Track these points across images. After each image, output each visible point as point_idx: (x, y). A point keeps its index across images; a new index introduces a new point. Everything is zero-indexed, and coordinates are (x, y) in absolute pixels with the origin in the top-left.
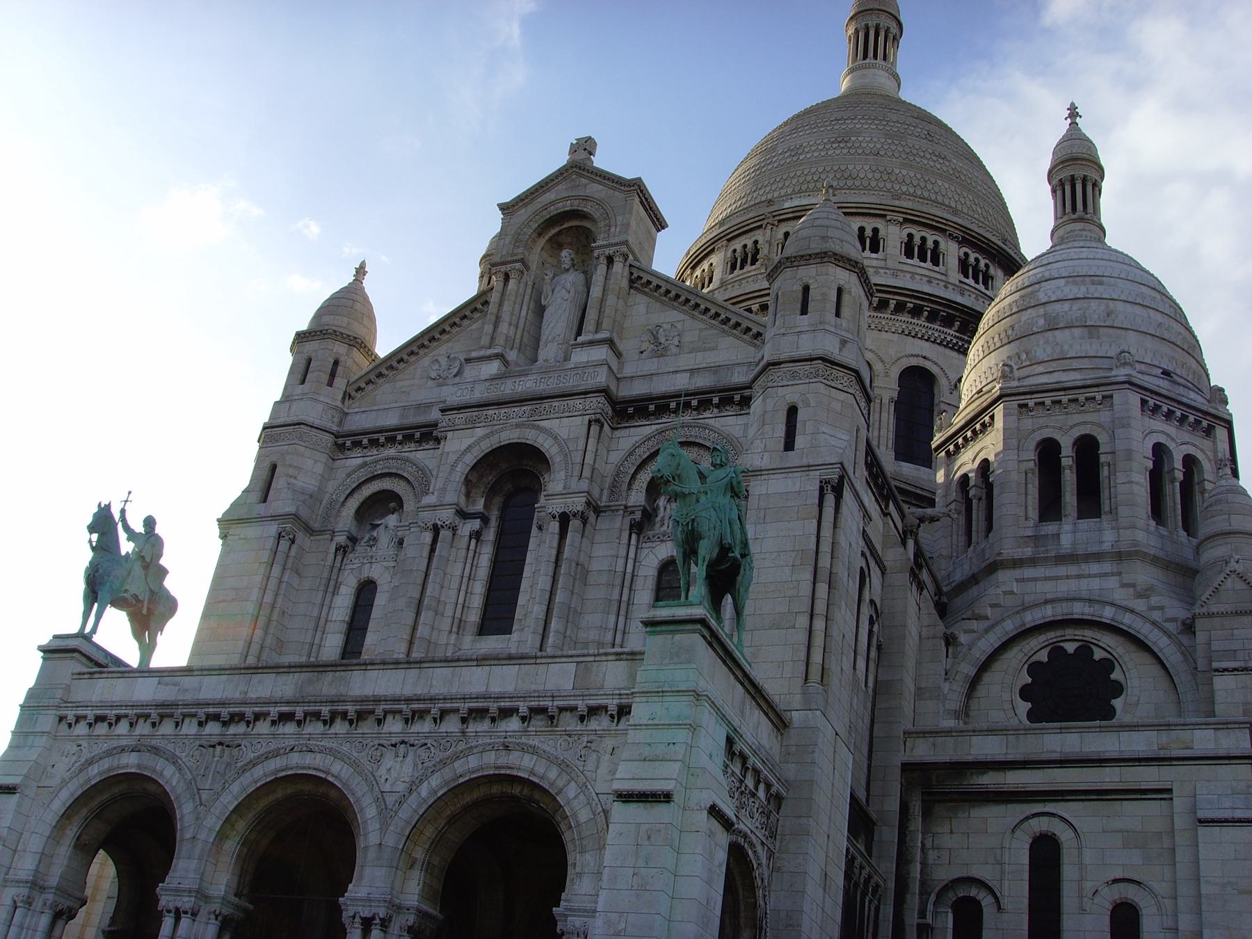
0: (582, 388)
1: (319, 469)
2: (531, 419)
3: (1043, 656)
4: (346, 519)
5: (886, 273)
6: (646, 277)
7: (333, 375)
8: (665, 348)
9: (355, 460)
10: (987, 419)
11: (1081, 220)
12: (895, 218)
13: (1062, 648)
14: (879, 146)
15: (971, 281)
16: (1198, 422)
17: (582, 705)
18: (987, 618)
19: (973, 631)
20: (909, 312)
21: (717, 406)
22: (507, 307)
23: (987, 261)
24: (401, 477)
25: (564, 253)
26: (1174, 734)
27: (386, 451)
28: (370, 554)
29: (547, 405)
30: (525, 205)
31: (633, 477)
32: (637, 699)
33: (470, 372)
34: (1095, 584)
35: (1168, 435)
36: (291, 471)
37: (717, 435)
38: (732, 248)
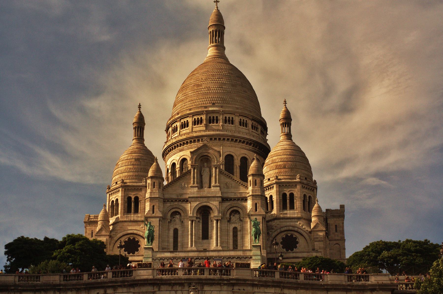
1: (162, 206)
3: (284, 236)
6: (223, 172)
7: (160, 187)
9: (168, 204)
10: (272, 187)
13: (288, 235)
15: (254, 131)
16: (311, 189)
17: (245, 257)
18: (274, 229)
19: (271, 231)
20: (242, 142)
23: (257, 124)
24: (179, 208)
25: (205, 164)
26: (310, 253)
31: (227, 212)
35: (306, 192)
38: (194, 118)
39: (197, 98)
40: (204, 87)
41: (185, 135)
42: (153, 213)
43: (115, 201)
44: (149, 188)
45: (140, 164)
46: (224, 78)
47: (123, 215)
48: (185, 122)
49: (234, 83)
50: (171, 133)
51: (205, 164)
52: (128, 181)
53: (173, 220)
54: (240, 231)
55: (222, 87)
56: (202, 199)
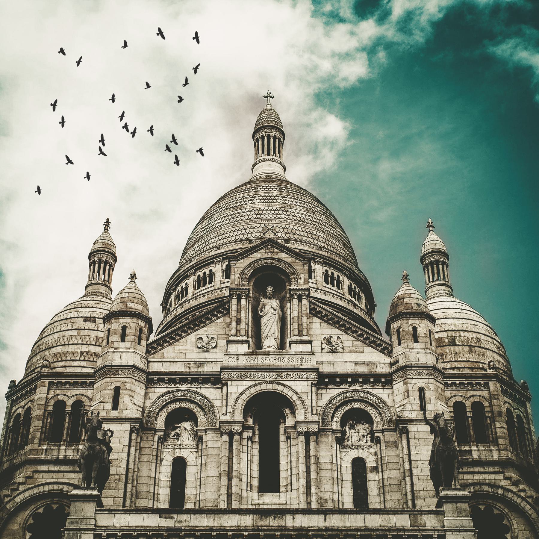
0: (304, 366)
1: (143, 393)
2: (277, 379)
4: (160, 423)
5: (321, 292)
6: (318, 309)
8: (336, 349)
9: (161, 390)
11: (444, 285)
12: (319, 260)
14: (304, 216)
15: (353, 300)
21: (372, 383)
22: (243, 314)
27: (180, 386)
28: (178, 443)
29: (285, 373)
30: (244, 258)
32: (447, 533)
33: (232, 348)
34: (492, 477)
36: (131, 393)
37: (375, 398)
39: (234, 229)
40: (247, 210)
41: (204, 296)
42: (115, 407)
43: (22, 413)
44: (108, 343)
45: (96, 328)
46: (290, 197)
47: (39, 447)
48: (205, 273)
49: (310, 208)
50: (173, 303)
51: (270, 288)
52: (61, 364)
53: (173, 433)
54: (375, 469)
55: (286, 210)
56: (260, 373)
